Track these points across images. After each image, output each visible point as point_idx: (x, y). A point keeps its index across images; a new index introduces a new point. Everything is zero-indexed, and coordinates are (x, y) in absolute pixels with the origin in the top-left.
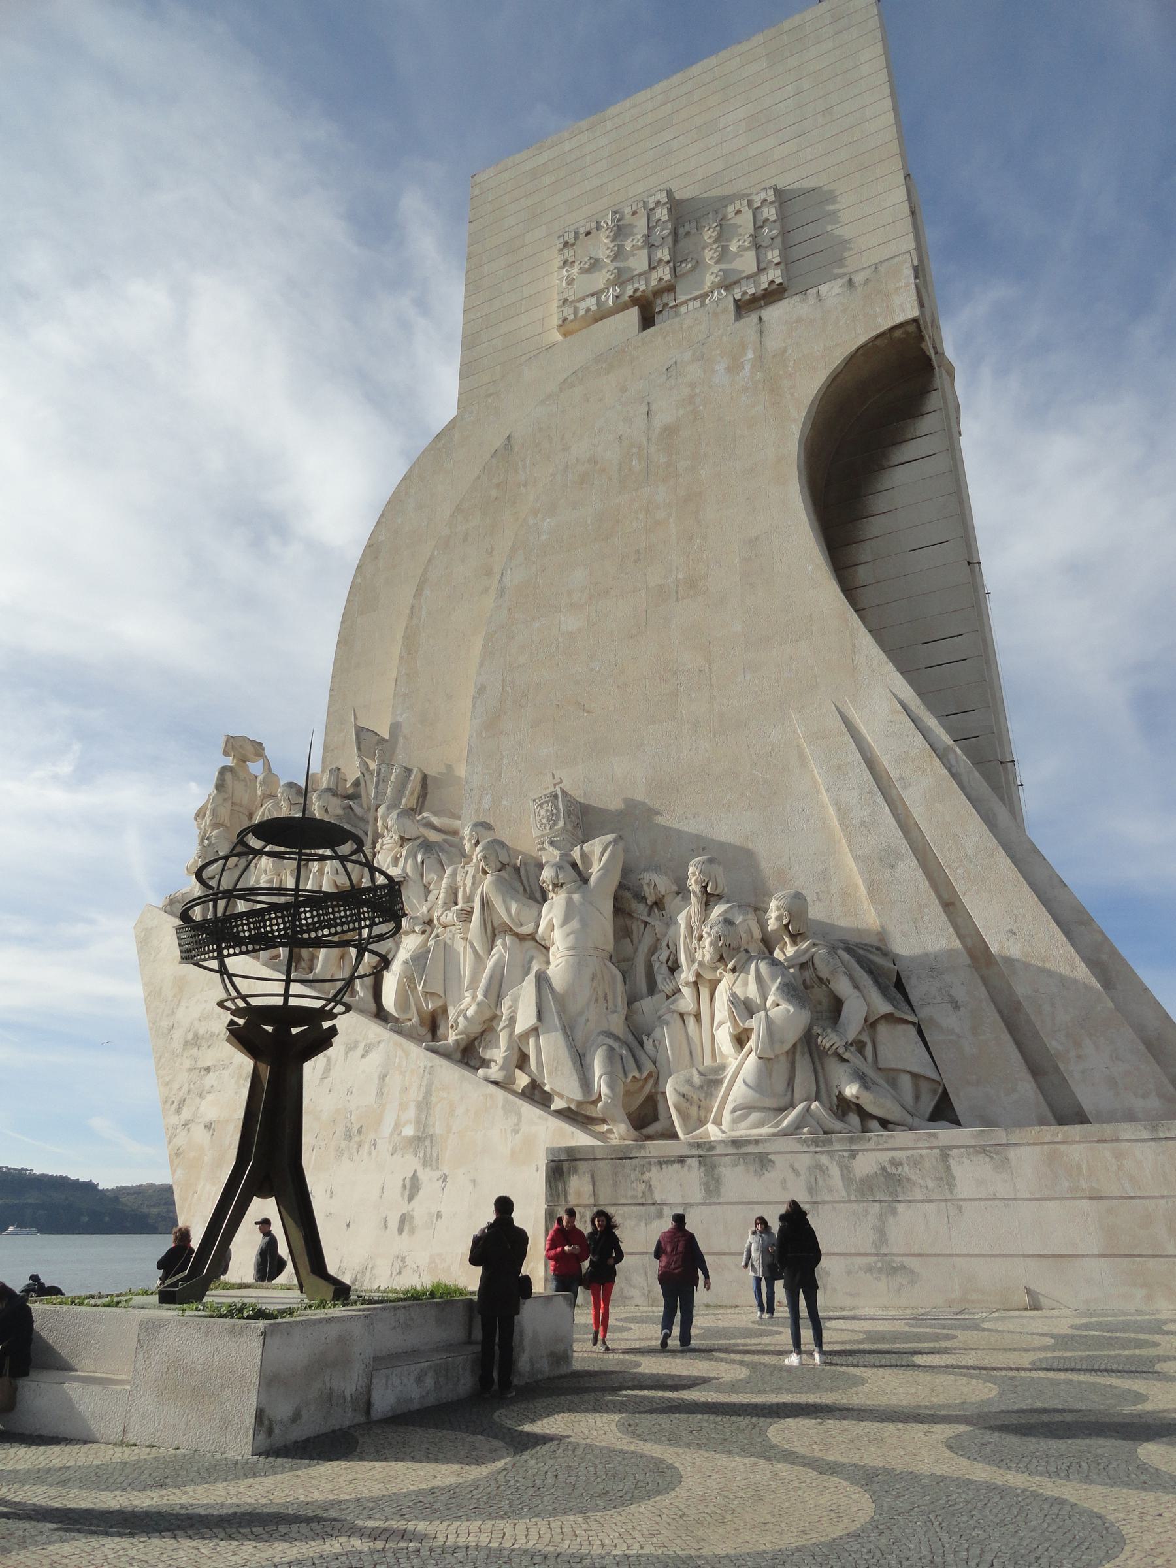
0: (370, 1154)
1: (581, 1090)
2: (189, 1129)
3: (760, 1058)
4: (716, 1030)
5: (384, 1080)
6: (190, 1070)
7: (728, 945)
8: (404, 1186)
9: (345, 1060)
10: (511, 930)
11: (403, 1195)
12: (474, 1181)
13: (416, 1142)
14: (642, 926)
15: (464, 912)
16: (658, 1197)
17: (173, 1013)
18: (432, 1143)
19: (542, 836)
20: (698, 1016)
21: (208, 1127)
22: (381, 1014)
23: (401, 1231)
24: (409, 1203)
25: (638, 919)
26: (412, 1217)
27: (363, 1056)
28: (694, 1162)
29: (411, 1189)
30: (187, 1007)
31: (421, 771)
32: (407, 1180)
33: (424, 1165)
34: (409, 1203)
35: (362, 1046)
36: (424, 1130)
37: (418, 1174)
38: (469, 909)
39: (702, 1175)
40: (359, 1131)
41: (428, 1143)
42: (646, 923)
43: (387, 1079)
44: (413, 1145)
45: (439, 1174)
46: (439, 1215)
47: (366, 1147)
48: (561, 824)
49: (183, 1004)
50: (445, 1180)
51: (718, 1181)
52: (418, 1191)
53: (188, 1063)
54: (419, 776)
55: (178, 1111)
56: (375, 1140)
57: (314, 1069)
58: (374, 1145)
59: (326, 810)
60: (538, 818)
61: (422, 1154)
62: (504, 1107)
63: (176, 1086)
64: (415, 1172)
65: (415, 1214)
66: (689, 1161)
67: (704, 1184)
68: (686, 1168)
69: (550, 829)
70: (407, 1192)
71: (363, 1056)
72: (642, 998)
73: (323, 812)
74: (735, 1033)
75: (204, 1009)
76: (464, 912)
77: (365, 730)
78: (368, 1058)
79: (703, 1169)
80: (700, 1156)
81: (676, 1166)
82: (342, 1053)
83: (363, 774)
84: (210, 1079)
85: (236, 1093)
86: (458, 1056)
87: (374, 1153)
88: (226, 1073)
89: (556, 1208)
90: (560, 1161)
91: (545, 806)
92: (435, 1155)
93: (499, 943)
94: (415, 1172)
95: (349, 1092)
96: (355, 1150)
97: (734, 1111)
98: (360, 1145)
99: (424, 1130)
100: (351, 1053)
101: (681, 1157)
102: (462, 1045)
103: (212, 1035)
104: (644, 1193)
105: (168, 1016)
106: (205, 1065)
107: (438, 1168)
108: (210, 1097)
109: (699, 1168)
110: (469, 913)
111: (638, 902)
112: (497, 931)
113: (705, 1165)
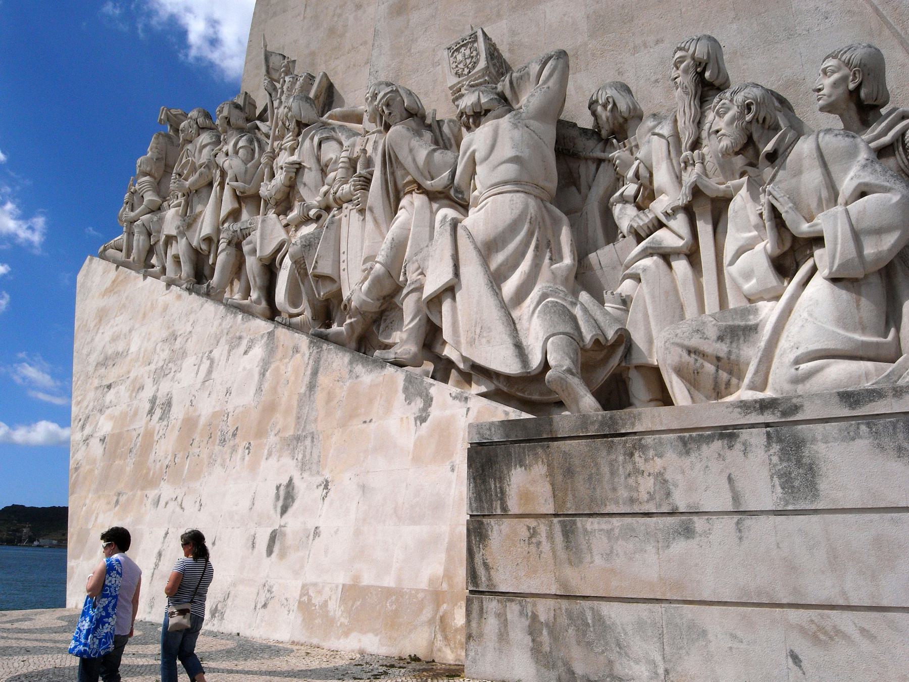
0: (244, 459)
1: (518, 360)
2: (88, 444)
3: (835, 280)
4: (732, 263)
5: (264, 375)
6: (97, 388)
7: (761, 121)
8: (277, 497)
9: (228, 359)
10: (420, 187)
11: (275, 507)
12: (363, 488)
13: (295, 442)
14: (593, 167)
15: (362, 179)
16: (681, 501)
17: (93, 340)
18: (313, 441)
19: (459, 83)
20: (692, 255)
21: (103, 440)
22: (272, 313)
23: (270, 552)
24: (281, 516)
25: (586, 159)
26: (284, 535)
27: (246, 353)
28: (757, 438)
29: (286, 499)
30: (103, 333)
31: (325, 75)
32: (282, 488)
33: (302, 470)
34: (281, 516)
35: (244, 343)
36: (305, 427)
37: (297, 482)
38: (369, 176)
39: (775, 459)
40: (234, 435)
41: (308, 442)
42: (600, 161)
43: (268, 374)
44: (291, 447)
45: (320, 479)
46: (317, 532)
47: (240, 451)
48: (482, 64)
49: (101, 331)
50: (326, 487)
51: (811, 471)
52: (293, 502)
53: (96, 382)
54: (325, 84)
55: (83, 428)
56: (250, 443)
57: (197, 373)
58: (248, 448)
59: (229, 123)
60: (454, 65)
61: (300, 456)
62: (406, 389)
63: (85, 403)
64: (291, 480)
65: (288, 530)
66: (745, 434)
67: (780, 476)
68: (738, 446)
69: (469, 72)
70: (280, 503)
71: (246, 353)
72: (596, 249)
73: (225, 125)
74: (778, 252)
75: (114, 333)
76: (362, 179)
77: (273, 55)
78: (251, 353)
79: (776, 448)
80: (767, 425)
81: (717, 444)
82: (226, 352)
83: (270, 95)
84: (110, 396)
85: (128, 406)
86: (353, 345)
87: (247, 458)
88: (122, 388)
89: (485, 520)
90: (492, 443)
91: (462, 49)
92: (315, 456)
93: (404, 202)
94: (291, 480)
95: (228, 392)
96: (227, 456)
97: (798, 361)
98: (234, 449)
99: (305, 427)
100: (234, 351)
101: (726, 427)
102: (358, 330)
103: (118, 353)
104: (651, 497)
105: (88, 344)
106: (108, 383)
107: (318, 472)
108: (108, 412)
109: (768, 445)
110: (366, 182)
111: (588, 139)
112: (402, 194)
113: (780, 441)
